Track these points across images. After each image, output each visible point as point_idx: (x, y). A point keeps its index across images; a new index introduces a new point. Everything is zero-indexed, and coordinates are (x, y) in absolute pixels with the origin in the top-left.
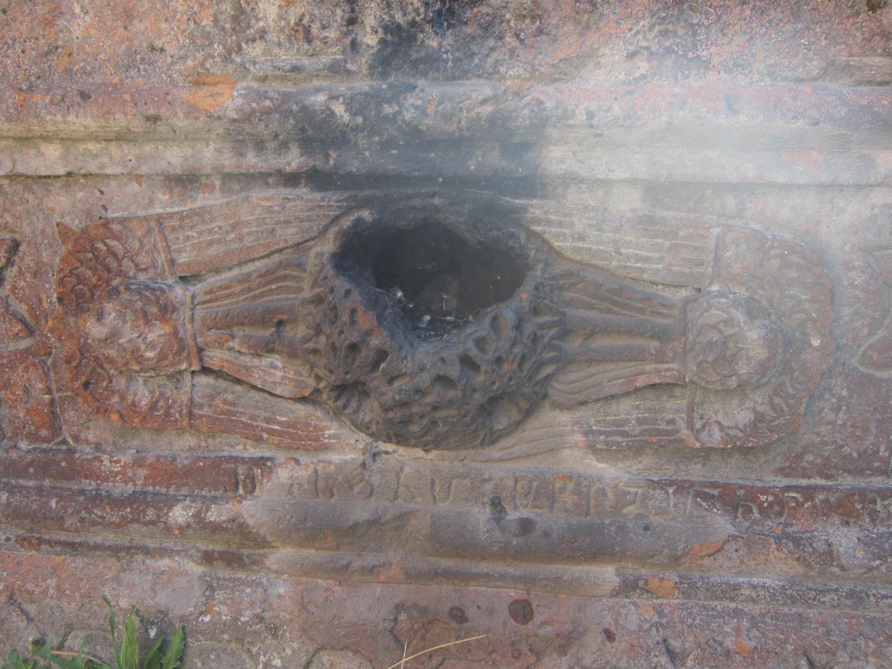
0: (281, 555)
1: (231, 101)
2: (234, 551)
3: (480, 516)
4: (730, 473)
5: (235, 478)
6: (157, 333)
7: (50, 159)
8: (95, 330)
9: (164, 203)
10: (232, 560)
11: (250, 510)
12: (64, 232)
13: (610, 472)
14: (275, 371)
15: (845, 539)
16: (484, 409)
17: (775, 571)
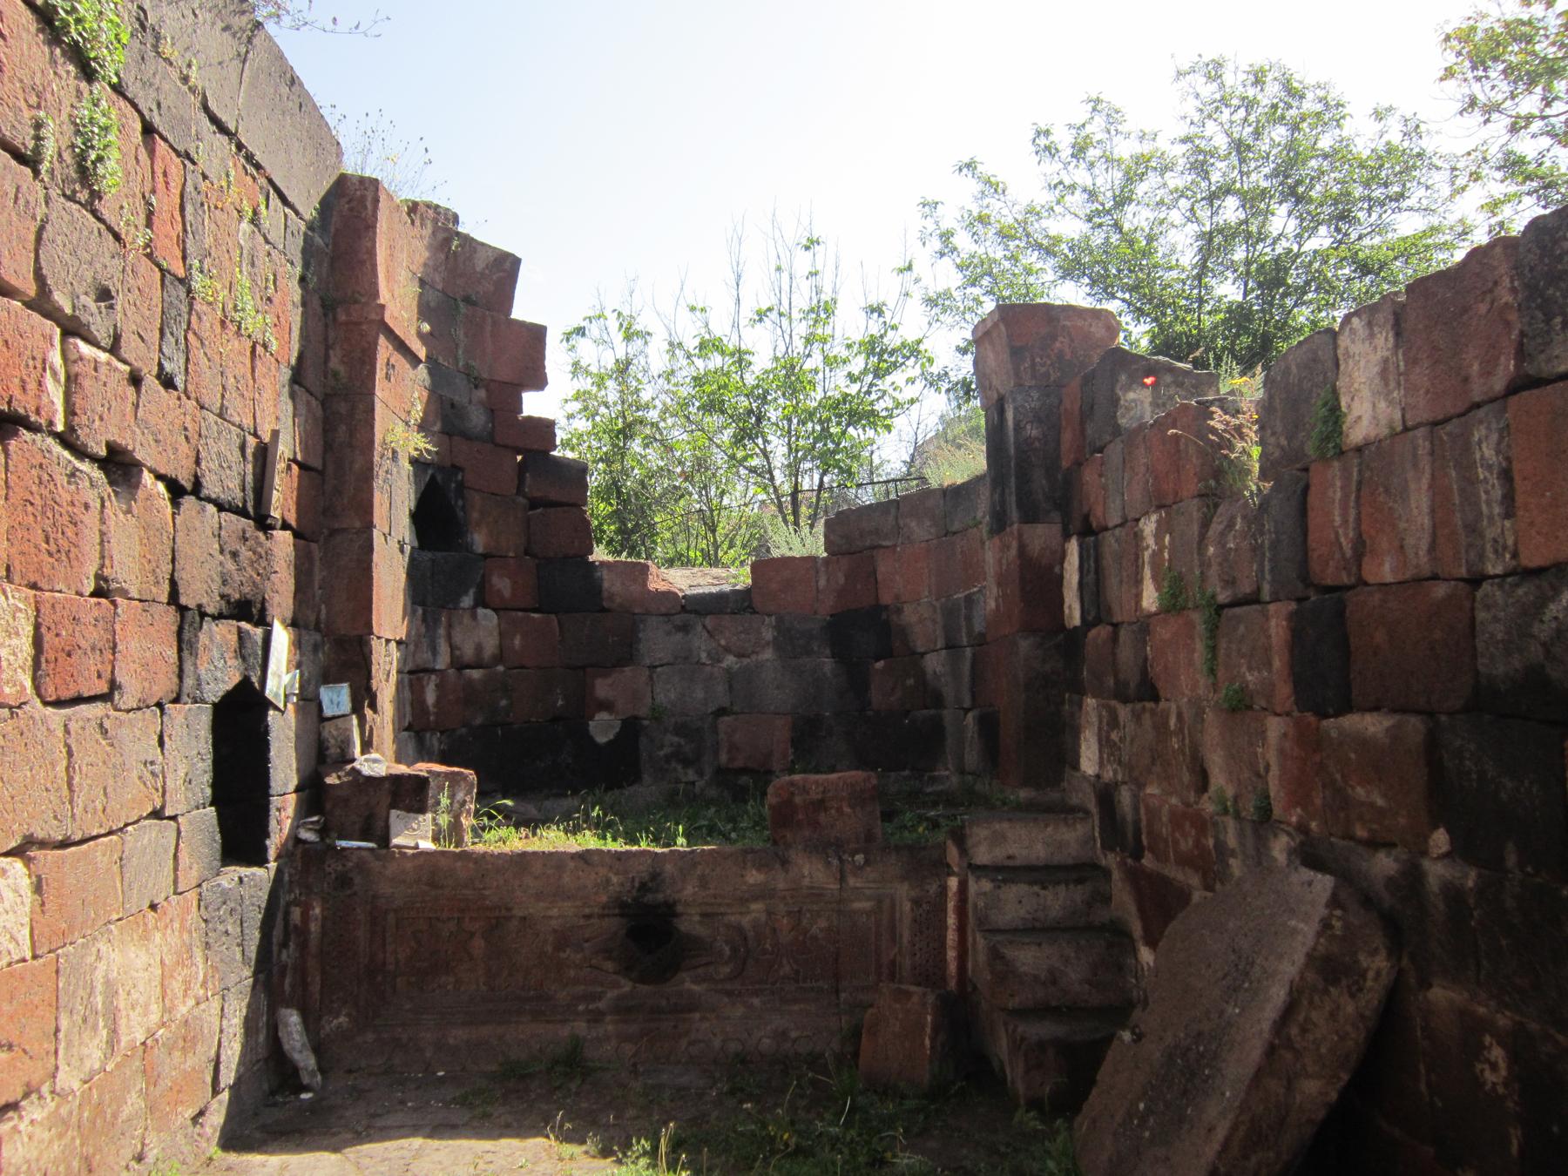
0: (608, 1018)
1: (604, 899)
2: (596, 1018)
3: (664, 1003)
4: (728, 986)
5: (597, 997)
6: (579, 956)
7: (555, 912)
8: (563, 955)
9: (582, 922)
10: (596, 1021)
11: (601, 1005)
12: (555, 931)
13: (695, 988)
14: (609, 966)
15: (756, 1001)
16: (662, 972)
17: (739, 1011)
